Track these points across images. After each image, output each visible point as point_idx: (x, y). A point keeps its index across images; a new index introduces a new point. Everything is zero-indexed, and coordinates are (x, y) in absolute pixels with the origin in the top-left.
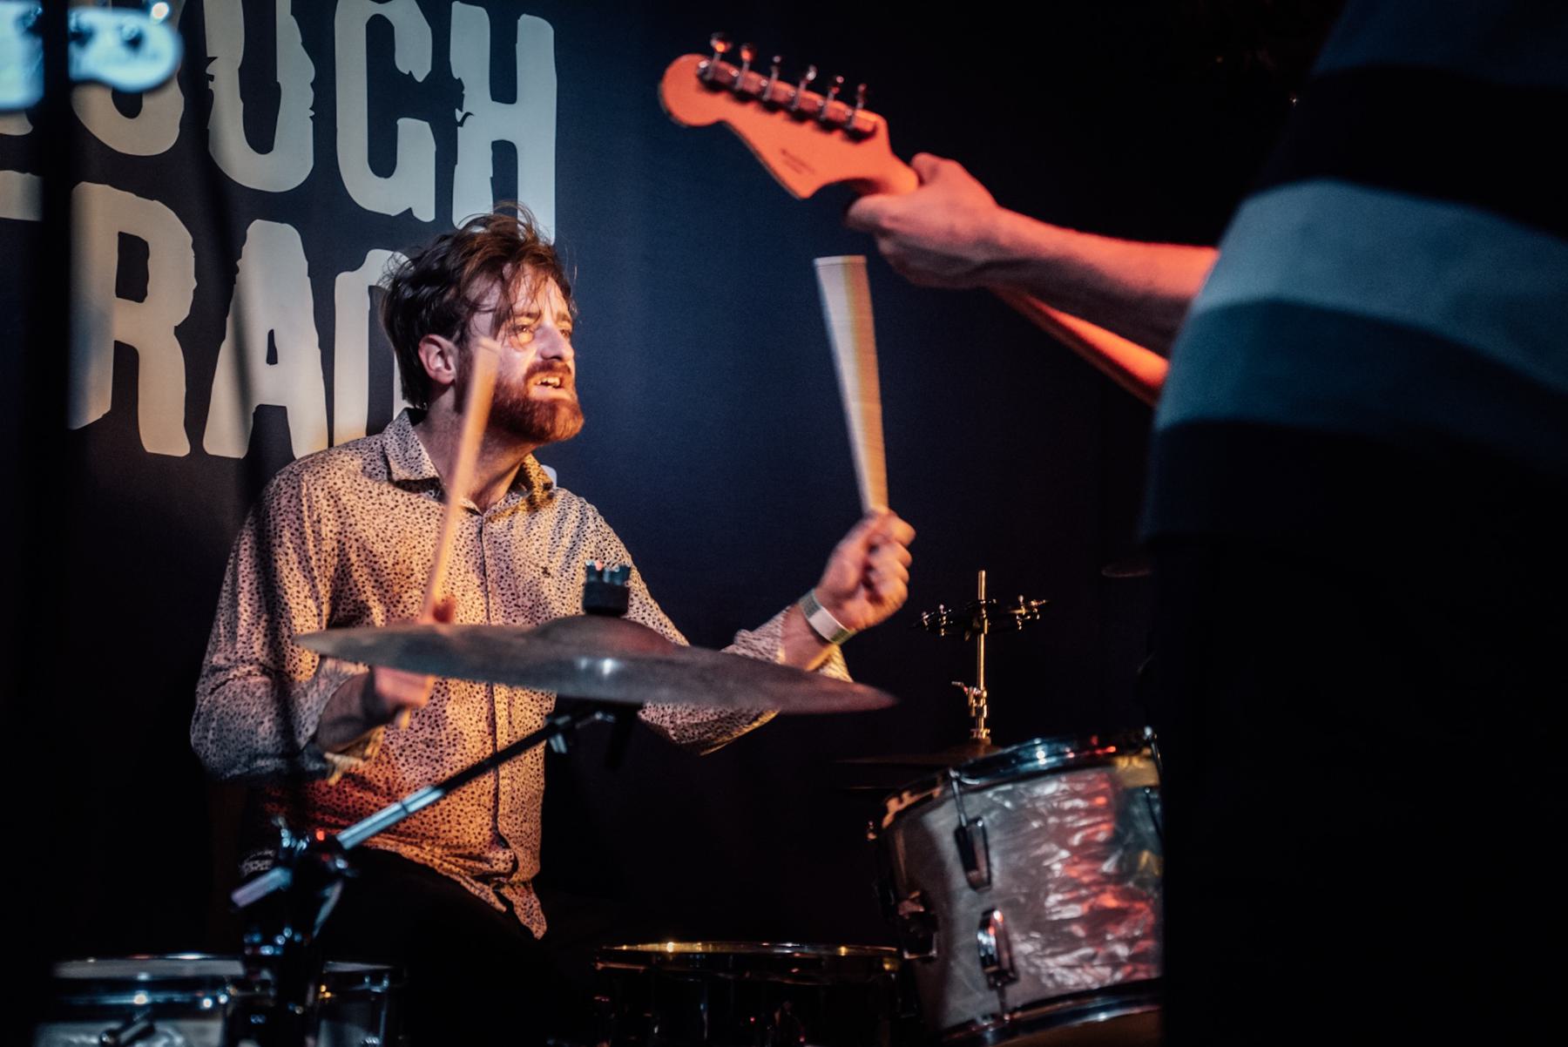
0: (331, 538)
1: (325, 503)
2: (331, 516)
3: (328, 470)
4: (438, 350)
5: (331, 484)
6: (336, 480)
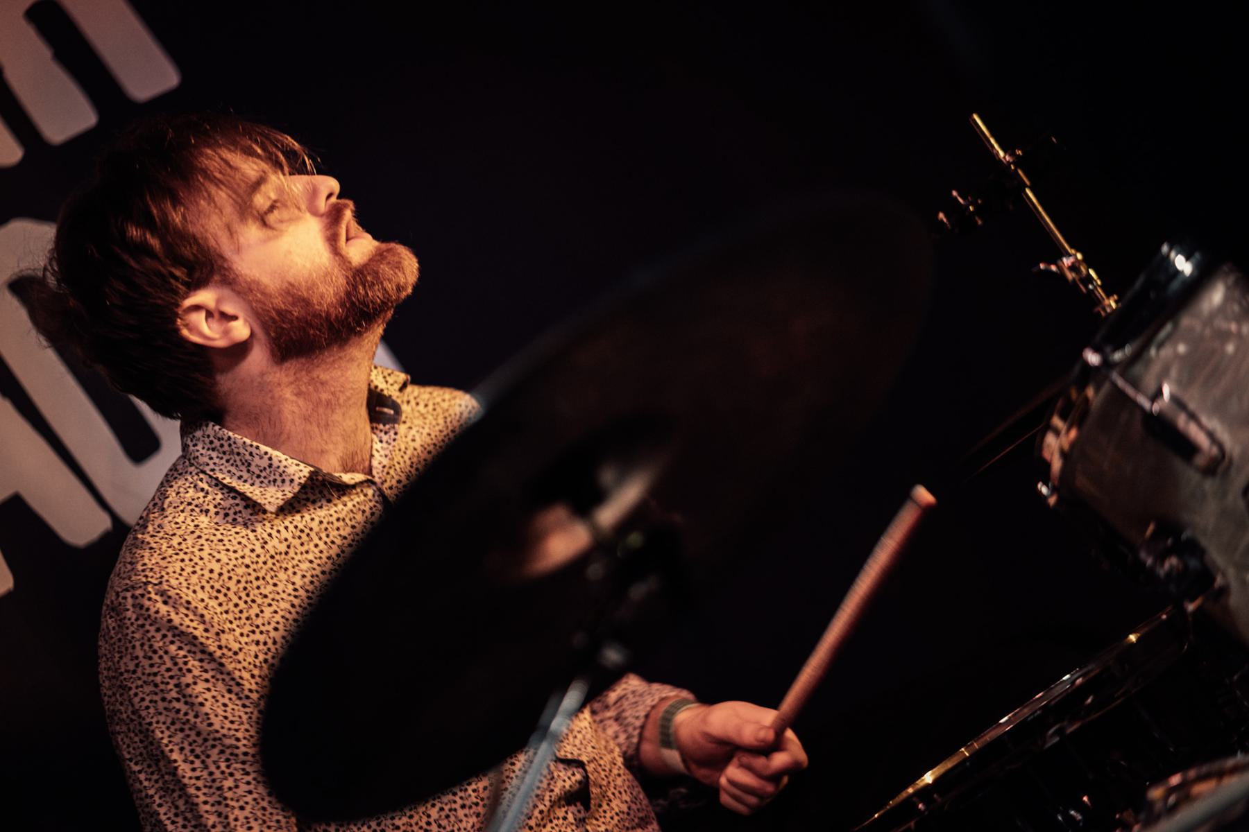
0: (246, 643)
1: (213, 603)
2: (230, 616)
3: (191, 560)
4: (203, 315)
5: (207, 575)
6: (210, 566)
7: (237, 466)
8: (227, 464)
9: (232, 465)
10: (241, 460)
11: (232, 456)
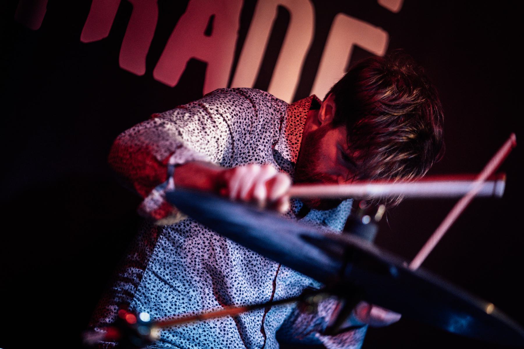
7: (290, 129)
8: (290, 125)
9: (290, 127)
10: (293, 131)
11: (294, 126)
